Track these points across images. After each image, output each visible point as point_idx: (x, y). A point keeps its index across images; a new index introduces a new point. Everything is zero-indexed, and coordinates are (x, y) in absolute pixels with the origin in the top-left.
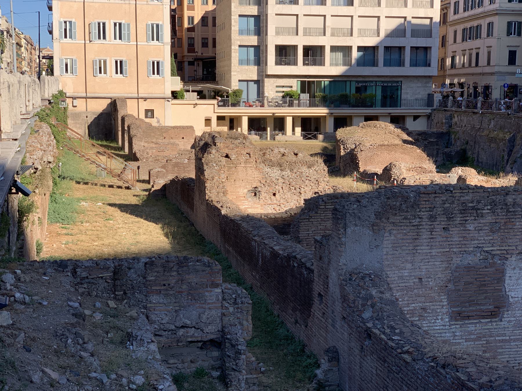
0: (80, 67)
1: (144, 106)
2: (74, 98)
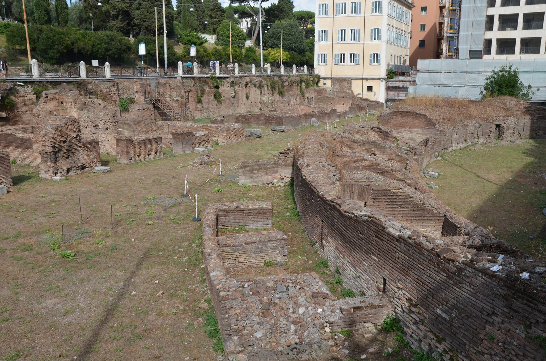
0: (329, 59)
1: (367, 84)
2: (325, 79)
